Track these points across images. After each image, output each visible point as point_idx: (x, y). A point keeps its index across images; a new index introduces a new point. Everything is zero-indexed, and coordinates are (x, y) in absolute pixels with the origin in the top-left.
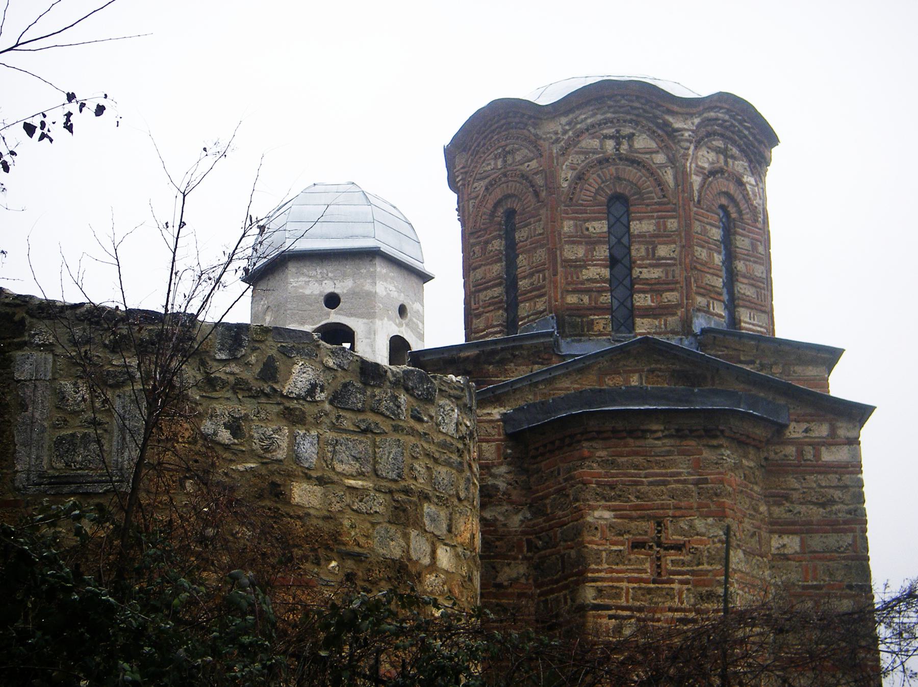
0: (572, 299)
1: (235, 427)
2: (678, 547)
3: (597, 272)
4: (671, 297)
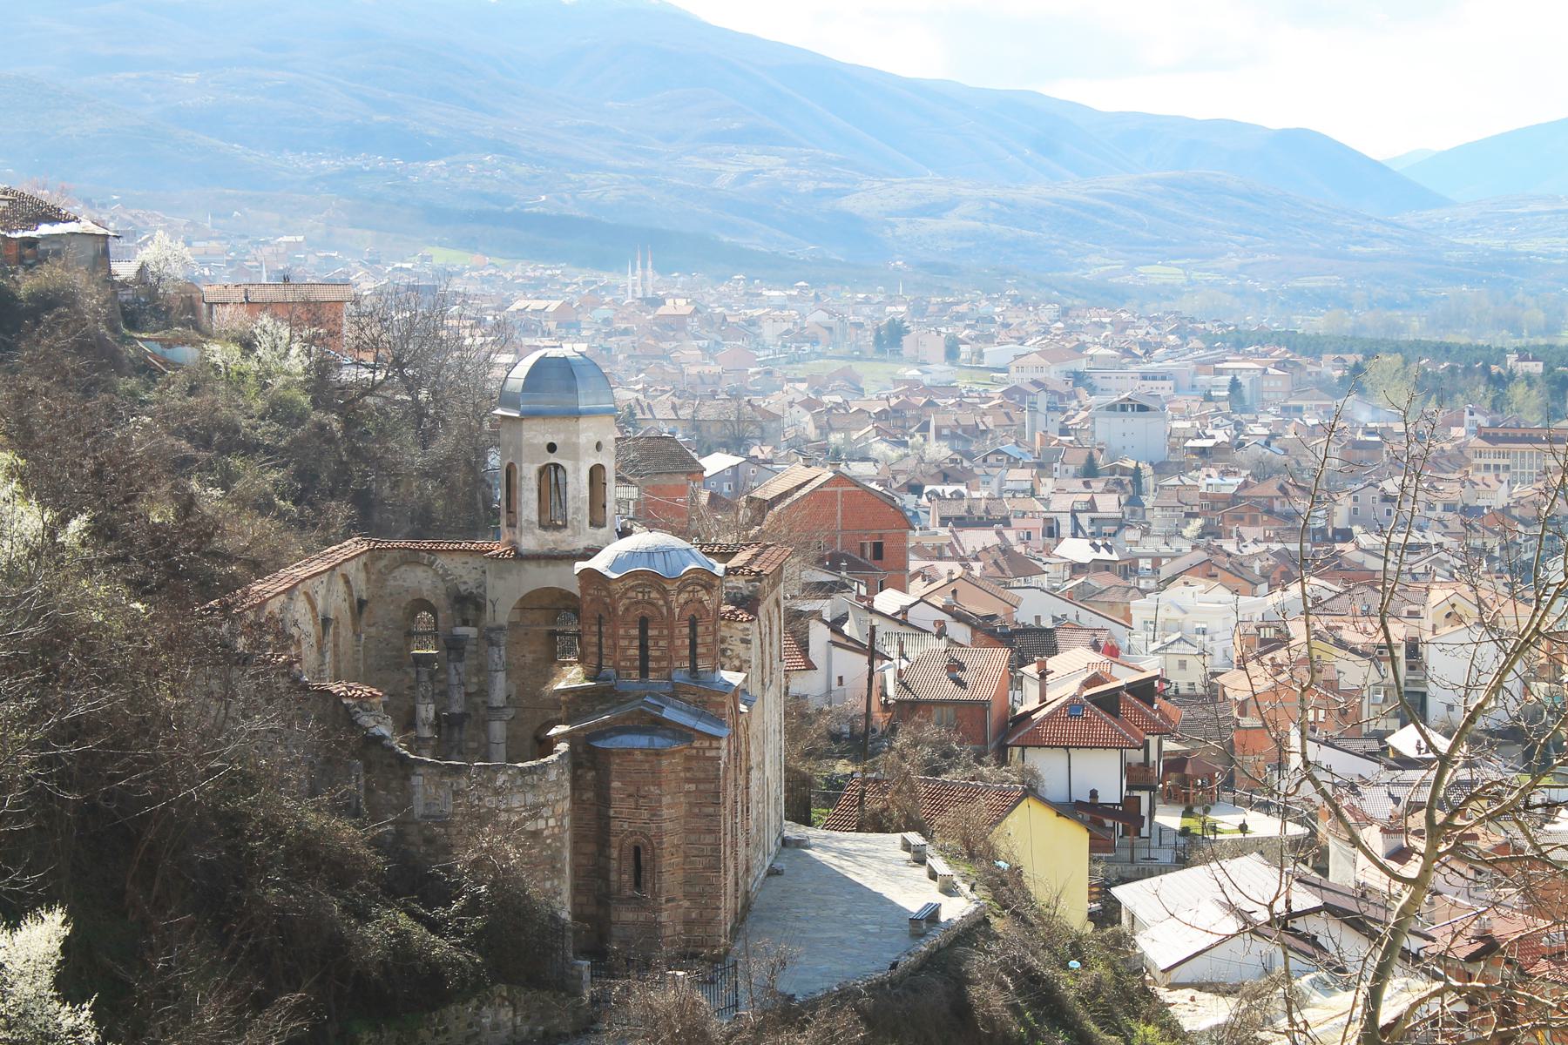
0: (623, 664)
1: (480, 799)
2: (644, 797)
3: (634, 652)
4: (664, 664)
